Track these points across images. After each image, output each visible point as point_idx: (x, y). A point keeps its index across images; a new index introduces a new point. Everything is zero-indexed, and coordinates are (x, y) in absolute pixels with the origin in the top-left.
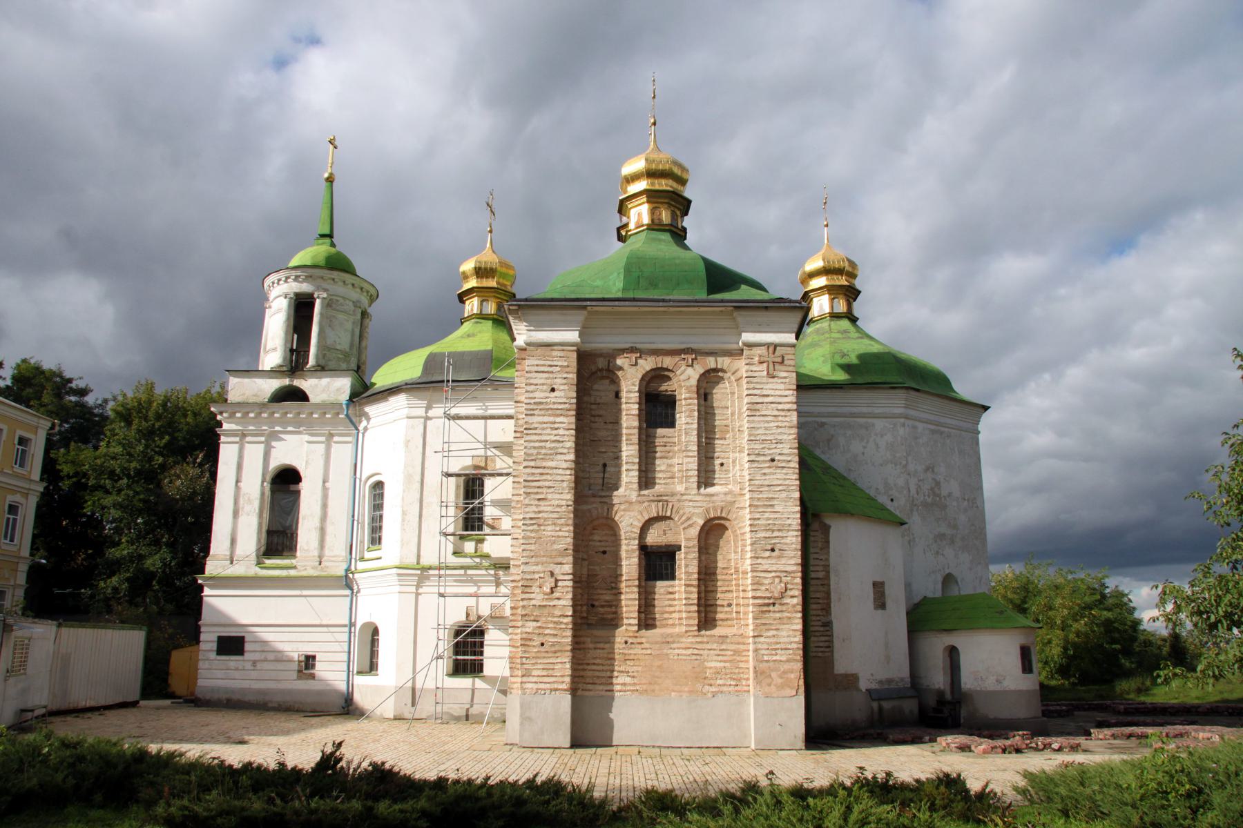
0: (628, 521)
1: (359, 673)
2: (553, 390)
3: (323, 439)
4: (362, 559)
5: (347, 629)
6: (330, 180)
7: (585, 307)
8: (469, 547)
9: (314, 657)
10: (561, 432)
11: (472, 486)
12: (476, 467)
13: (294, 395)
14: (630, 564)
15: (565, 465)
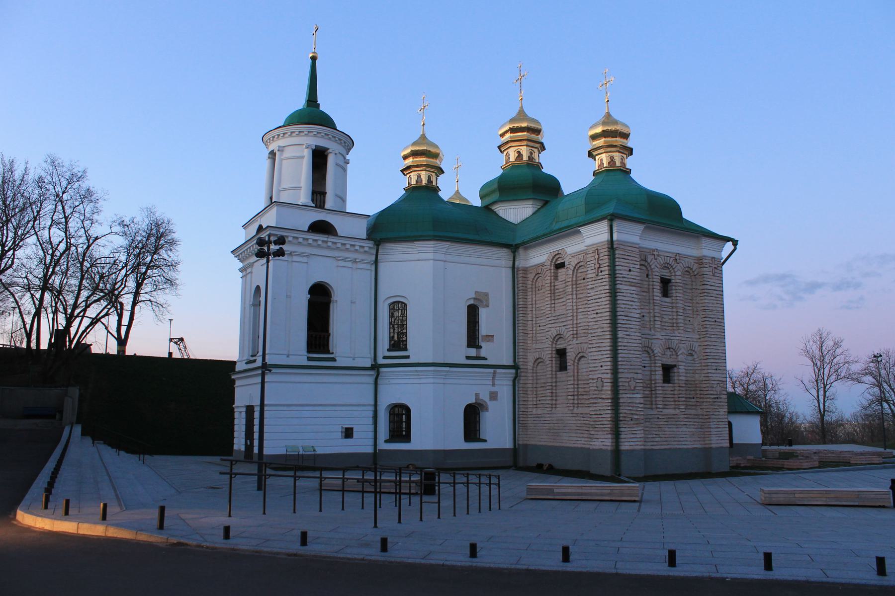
0: (658, 350)
1: (386, 441)
2: (630, 270)
3: (350, 264)
4: (385, 357)
5: (372, 408)
6: (314, 59)
7: (643, 223)
8: (473, 352)
9: (352, 429)
10: (635, 296)
11: (473, 313)
12: (475, 299)
13: (321, 228)
14: (659, 375)
15: (638, 316)
